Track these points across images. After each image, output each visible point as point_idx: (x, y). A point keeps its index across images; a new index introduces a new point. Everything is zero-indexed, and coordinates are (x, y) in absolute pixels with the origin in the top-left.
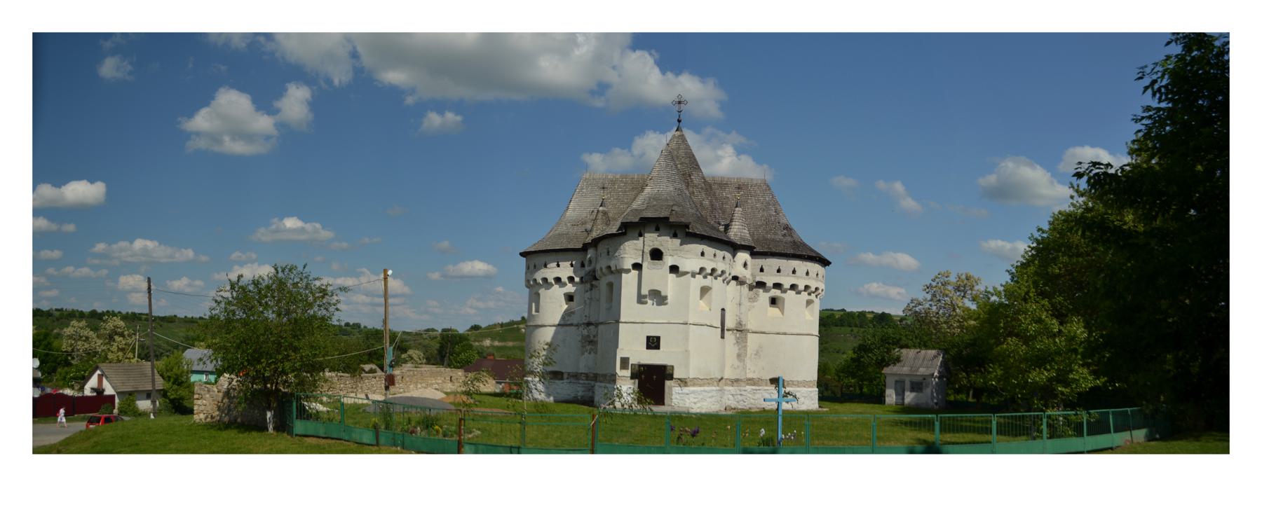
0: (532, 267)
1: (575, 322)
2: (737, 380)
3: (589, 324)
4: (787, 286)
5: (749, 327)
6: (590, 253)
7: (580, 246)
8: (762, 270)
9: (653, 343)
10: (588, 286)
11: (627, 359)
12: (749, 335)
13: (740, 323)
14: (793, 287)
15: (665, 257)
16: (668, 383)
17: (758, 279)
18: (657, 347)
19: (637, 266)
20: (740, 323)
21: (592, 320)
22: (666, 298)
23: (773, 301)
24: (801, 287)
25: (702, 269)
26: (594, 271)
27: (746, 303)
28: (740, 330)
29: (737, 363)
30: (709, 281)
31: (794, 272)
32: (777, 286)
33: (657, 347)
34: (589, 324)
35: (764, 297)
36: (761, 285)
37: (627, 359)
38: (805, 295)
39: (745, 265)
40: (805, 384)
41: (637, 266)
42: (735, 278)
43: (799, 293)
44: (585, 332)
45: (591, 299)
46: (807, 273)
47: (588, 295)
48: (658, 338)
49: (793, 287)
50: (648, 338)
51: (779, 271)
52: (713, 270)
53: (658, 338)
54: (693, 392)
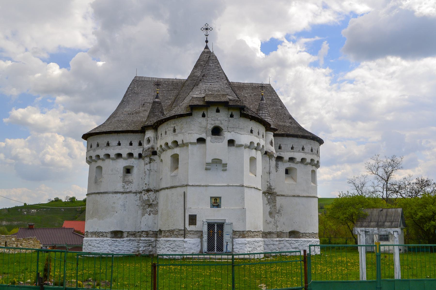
0: (94, 146)
1: (134, 190)
2: (270, 233)
3: (148, 191)
4: (299, 159)
6: (150, 134)
7: (139, 128)
8: (280, 148)
9: (216, 202)
10: (147, 160)
11: (195, 216)
12: (278, 198)
13: (270, 188)
18: (218, 206)
19: (201, 141)
20: (270, 188)
21: (151, 187)
22: (226, 164)
23: (287, 172)
24: (308, 161)
25: (252, 143)
26: (153, 148)
27: (273, 170)
29: (269, 219)
30: (253, 153)
31: (303, 149)
32: (291, 159)
34: (148, 191)
35: (283, 167)
36: (280, 159)
37: (195, 216)
38: (310, 168)
40: (312, 235)
41: (201, 141)
42: (266, 153)
43: (307, 164)
44: (145, 197)
45: (150, 170)
46: (312, 150)
47: (148, 167)
49: (303, 160)
52: (258, 144)
54: (249, 242)
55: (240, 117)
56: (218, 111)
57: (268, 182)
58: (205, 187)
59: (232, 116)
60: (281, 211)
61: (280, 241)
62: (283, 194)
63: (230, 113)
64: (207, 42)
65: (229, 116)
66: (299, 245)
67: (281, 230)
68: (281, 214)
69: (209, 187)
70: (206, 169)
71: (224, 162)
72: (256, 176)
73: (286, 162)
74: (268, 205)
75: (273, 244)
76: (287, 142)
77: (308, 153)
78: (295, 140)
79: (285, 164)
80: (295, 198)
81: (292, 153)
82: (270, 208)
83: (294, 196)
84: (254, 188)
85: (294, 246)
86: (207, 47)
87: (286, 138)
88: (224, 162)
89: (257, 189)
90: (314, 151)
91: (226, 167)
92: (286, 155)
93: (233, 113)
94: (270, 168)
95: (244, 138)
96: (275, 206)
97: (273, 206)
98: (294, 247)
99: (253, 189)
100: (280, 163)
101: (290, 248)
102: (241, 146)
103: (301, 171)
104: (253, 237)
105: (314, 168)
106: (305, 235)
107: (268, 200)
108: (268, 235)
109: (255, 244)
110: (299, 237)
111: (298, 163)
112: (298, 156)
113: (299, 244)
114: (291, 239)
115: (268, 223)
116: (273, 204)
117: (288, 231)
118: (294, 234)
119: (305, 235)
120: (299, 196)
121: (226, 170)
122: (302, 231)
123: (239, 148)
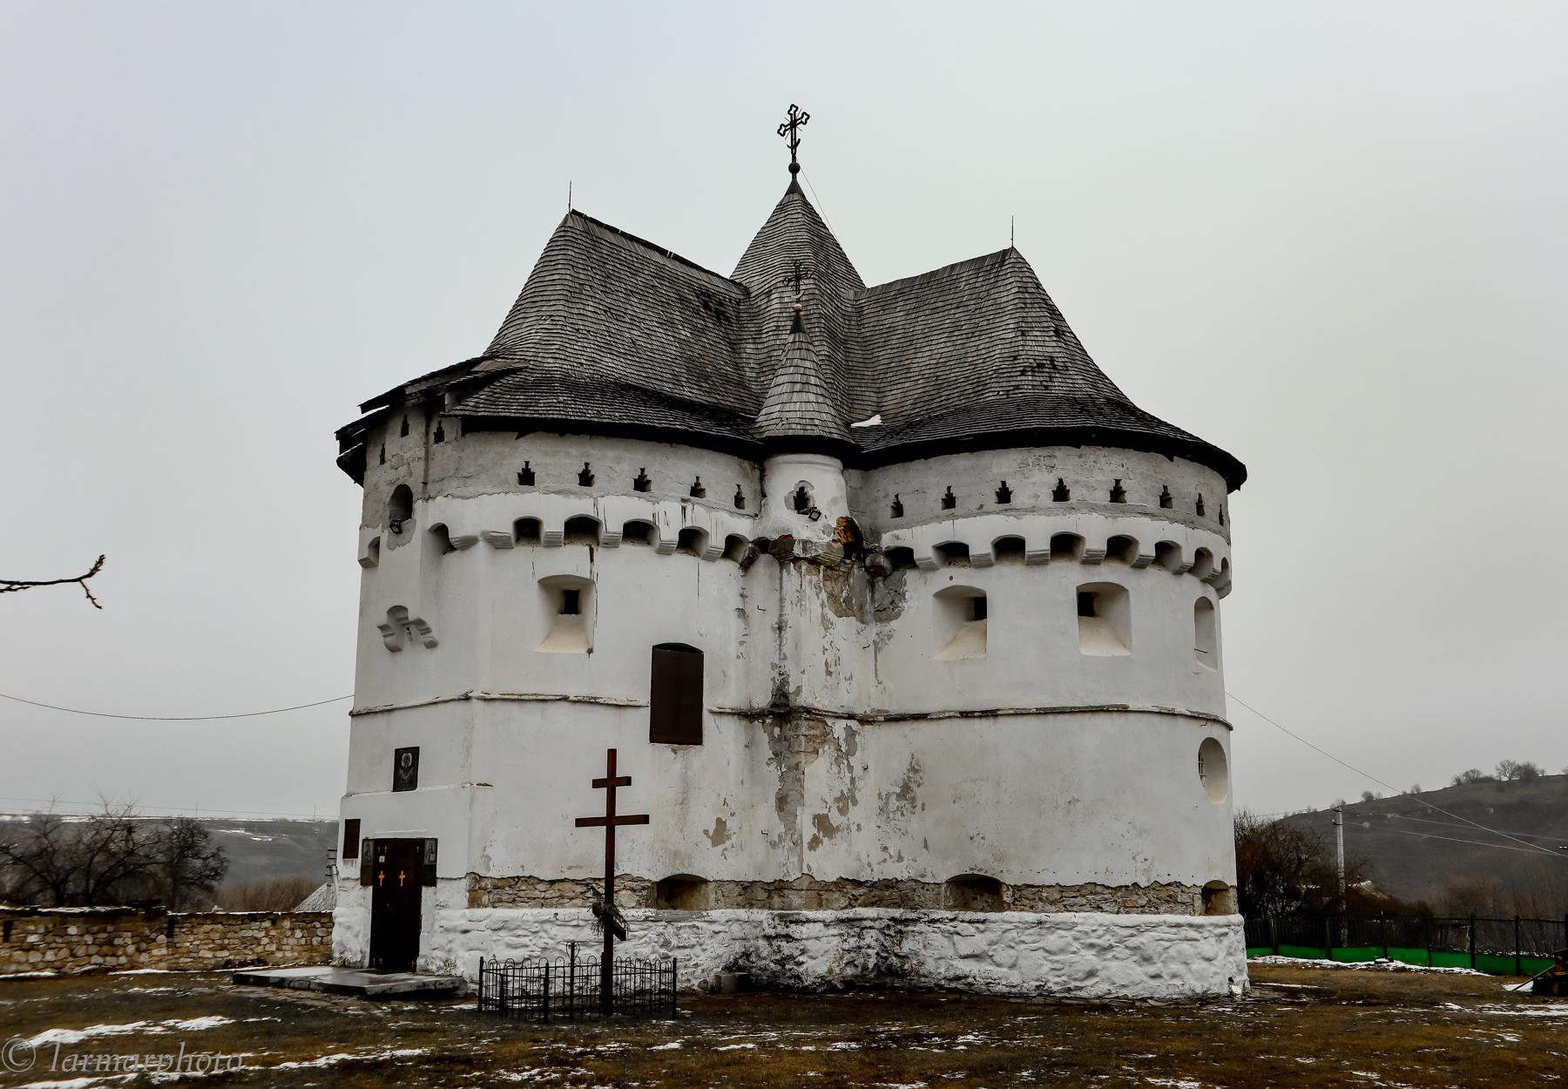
4: (980, 546)
5: (821, 702)
8: (898, 510)
14: (1009, 548)
15: (418, 506)
16: (426, 892)
17: (887, 541)
24: (1038, 543)
28: (782, 712)
30: (571, 560)
31: (1004, 495)
32: (954, 552)
33: (411, 784)
35: (920, 594)
36: (903, 558)
38: (1070, 576)
39: (801, 502)
42: (763, 545)
43: (1038, 561)
46: (1061, 494)
48: (415, 751)
50: (399, 753)
51: (949, 502)
53: (415, 751)
55: (463, 435)
56: (405, 432)
57: (774, 666)
58: (386, 716)
59: (440, 437)
60: (913, 786)
61: (906, 922)
62: (923, 710)
63: (434, 429)
64: (794, 169)
65: (432, 438)
66: (992, 943)
67: (913, 875)
68: (914, 799)
69: (397, 713)
70: (394, 650)
71: (412, 616)
72: (590, 651)
73: (931, 568)
74: (772, 768)
75: (788, 937)
76: (922, 482)
77: (1033, 510)
78: (962, 461)
79: (930, 575)
80: (977, 724)
81: (947, 524)
82: (782, 778)
83: (966, 715)
84: (565, 699)
85: (965, 947)
86: (794, 188)
87: (918, 465)
88: (412, 616)
89: (592, 702)
90: (1075, 494)
91: (428, 631)
92: (922, 539)
93: (445, 427)
94: (782, 608)
95: (483, 509)
96: (797, 767)
97: (789, 768)
98: (969, 951)
99: (564, 704)
100: (911, 576)
101: (950, 952)
102: (468, 543)
103: (1154, 599)
104: (544, 903)
105: (1109, 573)
106: (1028, 895)
107: (774, 741)
108: (776, 900)
109: (554, 930)
110: (1000, 906)
111: (983, 563)
112: (979, 533)
113: (990, 936)
114: (950, 915)
115: (773, 845)
116: (793, 761)
117: (943, 877)
118: (978, 890)
119: (1028, 895)
120: (991, 714)
121: (432, 645)
122: (1010, 876)
123: (468, 552)
